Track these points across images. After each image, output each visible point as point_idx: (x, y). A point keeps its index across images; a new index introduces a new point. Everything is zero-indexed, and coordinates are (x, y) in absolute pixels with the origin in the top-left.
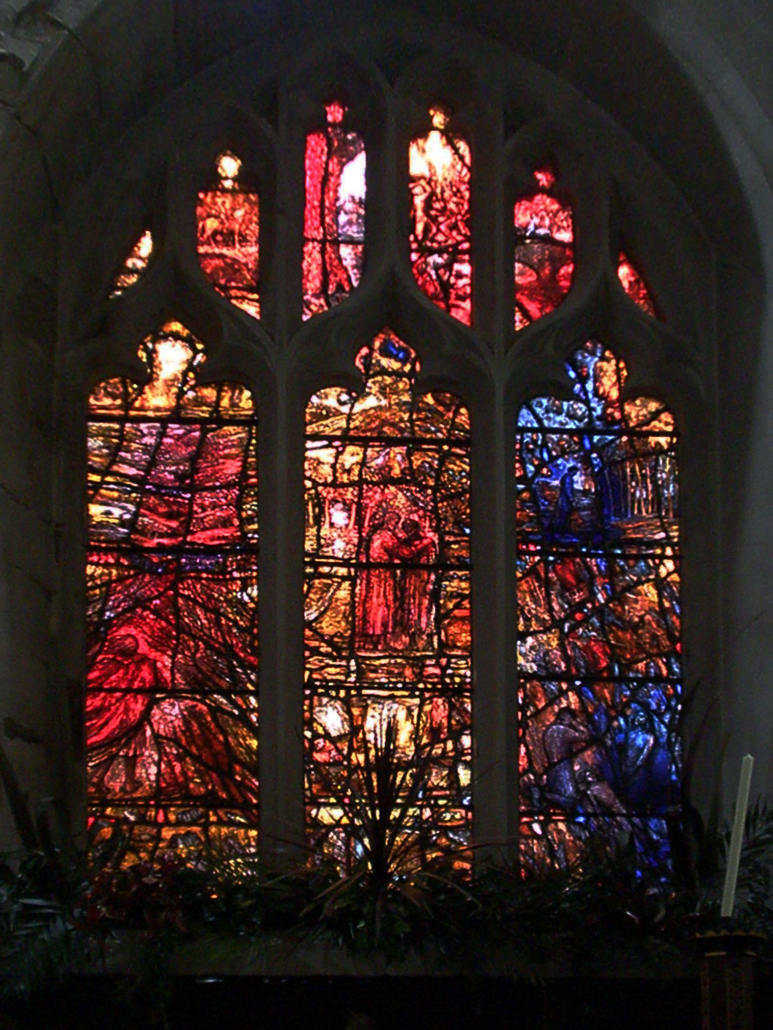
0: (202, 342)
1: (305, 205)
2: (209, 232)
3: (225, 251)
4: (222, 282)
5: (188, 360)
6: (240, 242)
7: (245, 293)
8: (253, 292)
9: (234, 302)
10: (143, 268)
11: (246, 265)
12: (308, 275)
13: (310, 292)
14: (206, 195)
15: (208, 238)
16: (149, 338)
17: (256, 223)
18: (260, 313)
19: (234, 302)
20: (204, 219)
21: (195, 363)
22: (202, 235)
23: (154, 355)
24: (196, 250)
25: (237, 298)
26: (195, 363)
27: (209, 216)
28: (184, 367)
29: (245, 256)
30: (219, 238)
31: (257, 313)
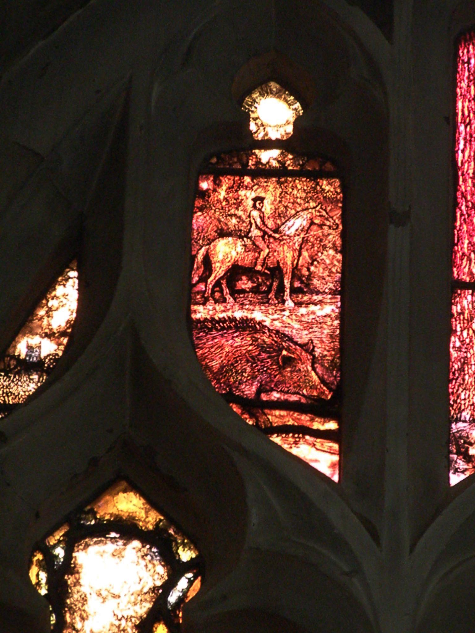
0: (194, 543)
1: (456, 205)
2: (219, 270)
3: (258, 315)
4: (250, 390)
5: (154, 589)
6: (294, 291)
7: (305, 419)
8: (326, 416)
9: (276, 439)
10: (55, 358)
11: (308, 347)
12: (461, 370)
13: (466, 415)
14: (217, 184)
15: (218, 284)
16: (59, 535)
17: (334, 247)
18: (341, 466)
19: (276, 439)
20: (210, 241)
21: (173, 598)
22: (203, 279)
23: (70, 580)
24: (189, 312)
25: (284, 430)
26: (173, 598)
27: (223, 233)
28: (143, 609)
29: (308, 326)
30: (245, 284)
31: (333, 466)
